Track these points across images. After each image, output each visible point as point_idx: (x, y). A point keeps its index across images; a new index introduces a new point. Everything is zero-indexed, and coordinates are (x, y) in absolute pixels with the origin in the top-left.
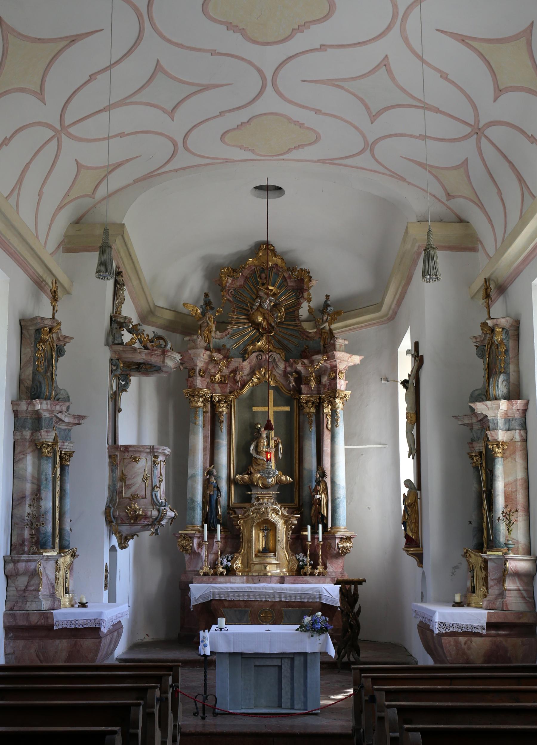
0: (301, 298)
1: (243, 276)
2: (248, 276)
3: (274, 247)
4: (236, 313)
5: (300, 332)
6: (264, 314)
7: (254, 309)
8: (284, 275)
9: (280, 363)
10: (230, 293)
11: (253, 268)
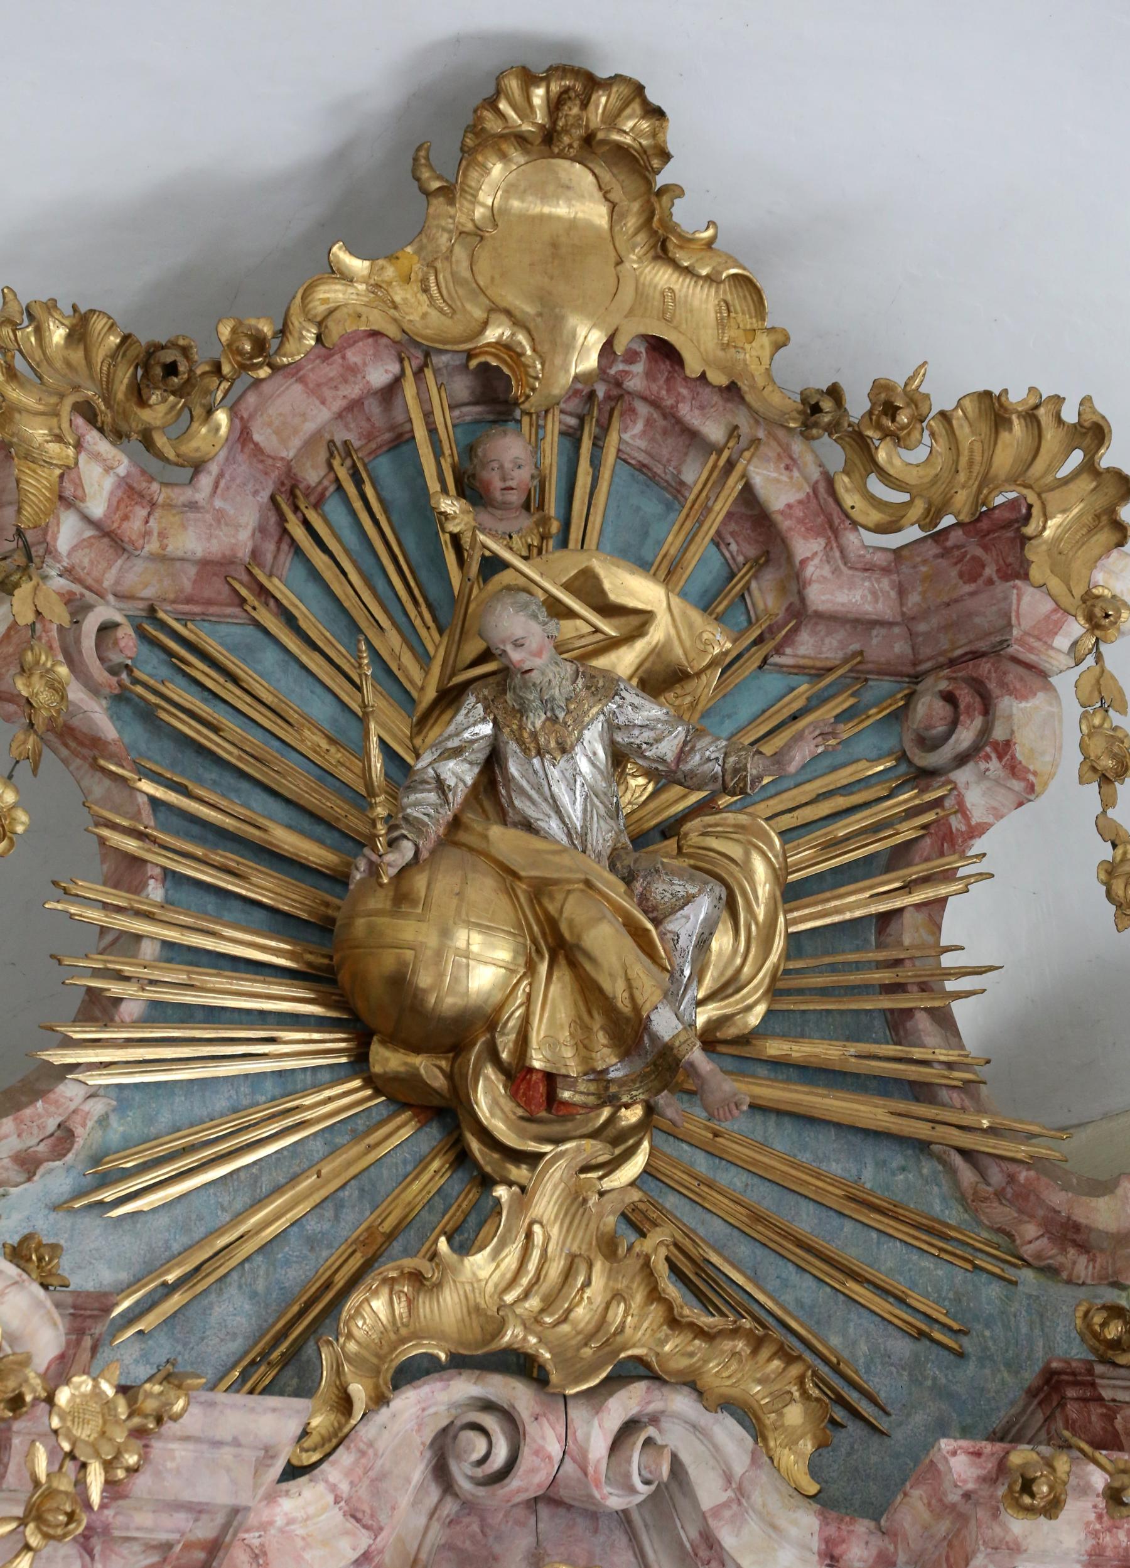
0: (962, 759)
1: (258, 450)
2: (312, 475)
3: (656, 113)
4: (155, 892)
5: (967, 1175)
6: (540, 890)
7: (416, 825)
8: (748, 494)
9: (753, 1527)
10: (88, 642)
11: (379, 375)
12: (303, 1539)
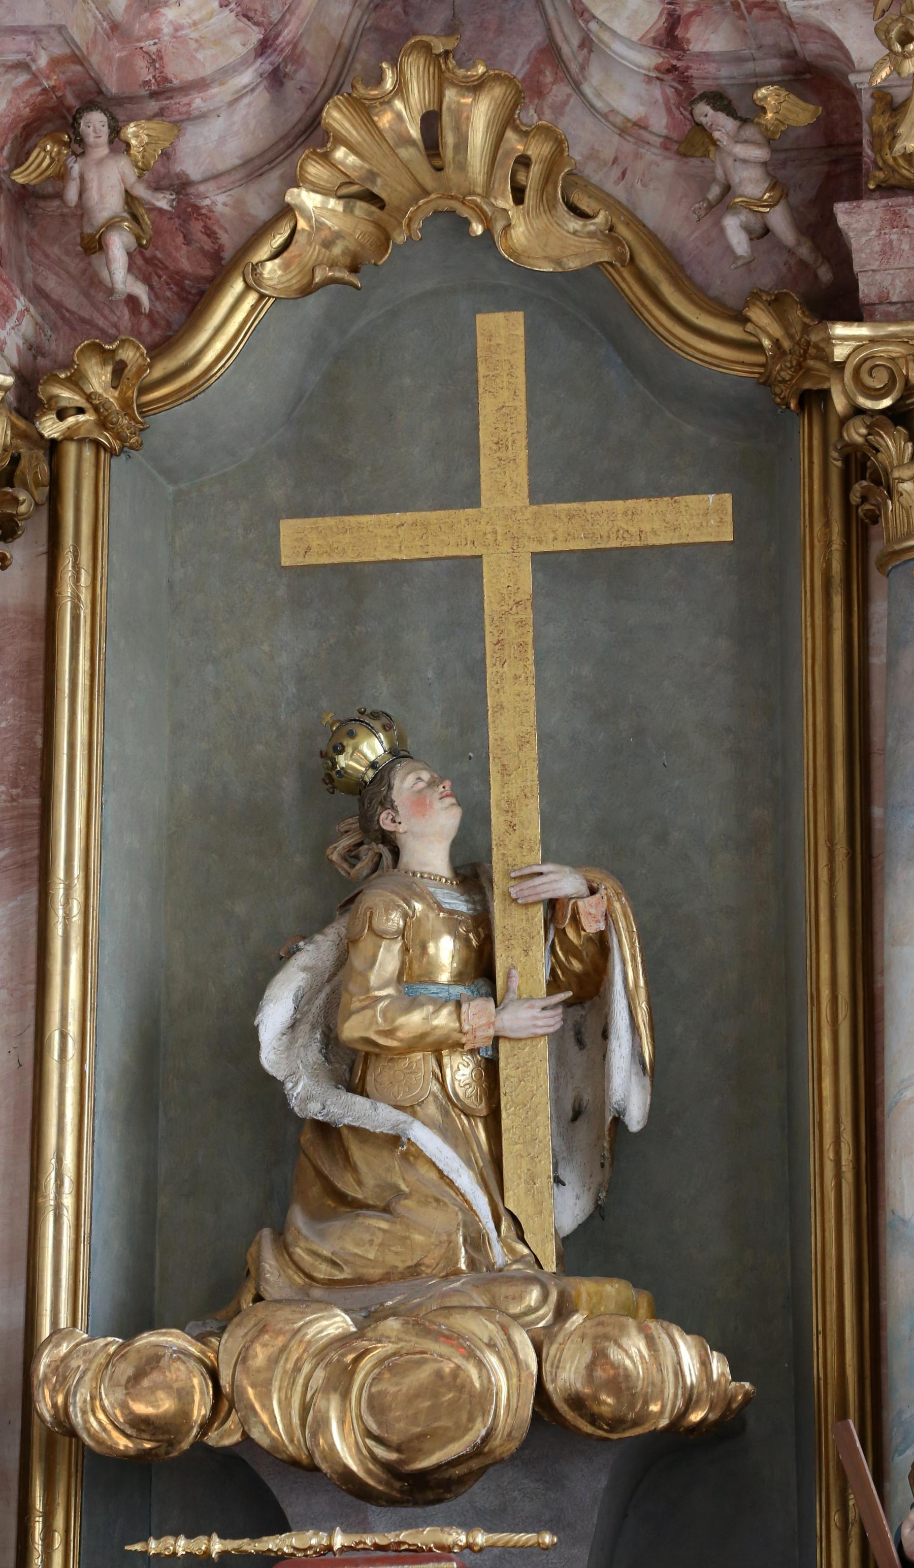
12: (197, 41)
